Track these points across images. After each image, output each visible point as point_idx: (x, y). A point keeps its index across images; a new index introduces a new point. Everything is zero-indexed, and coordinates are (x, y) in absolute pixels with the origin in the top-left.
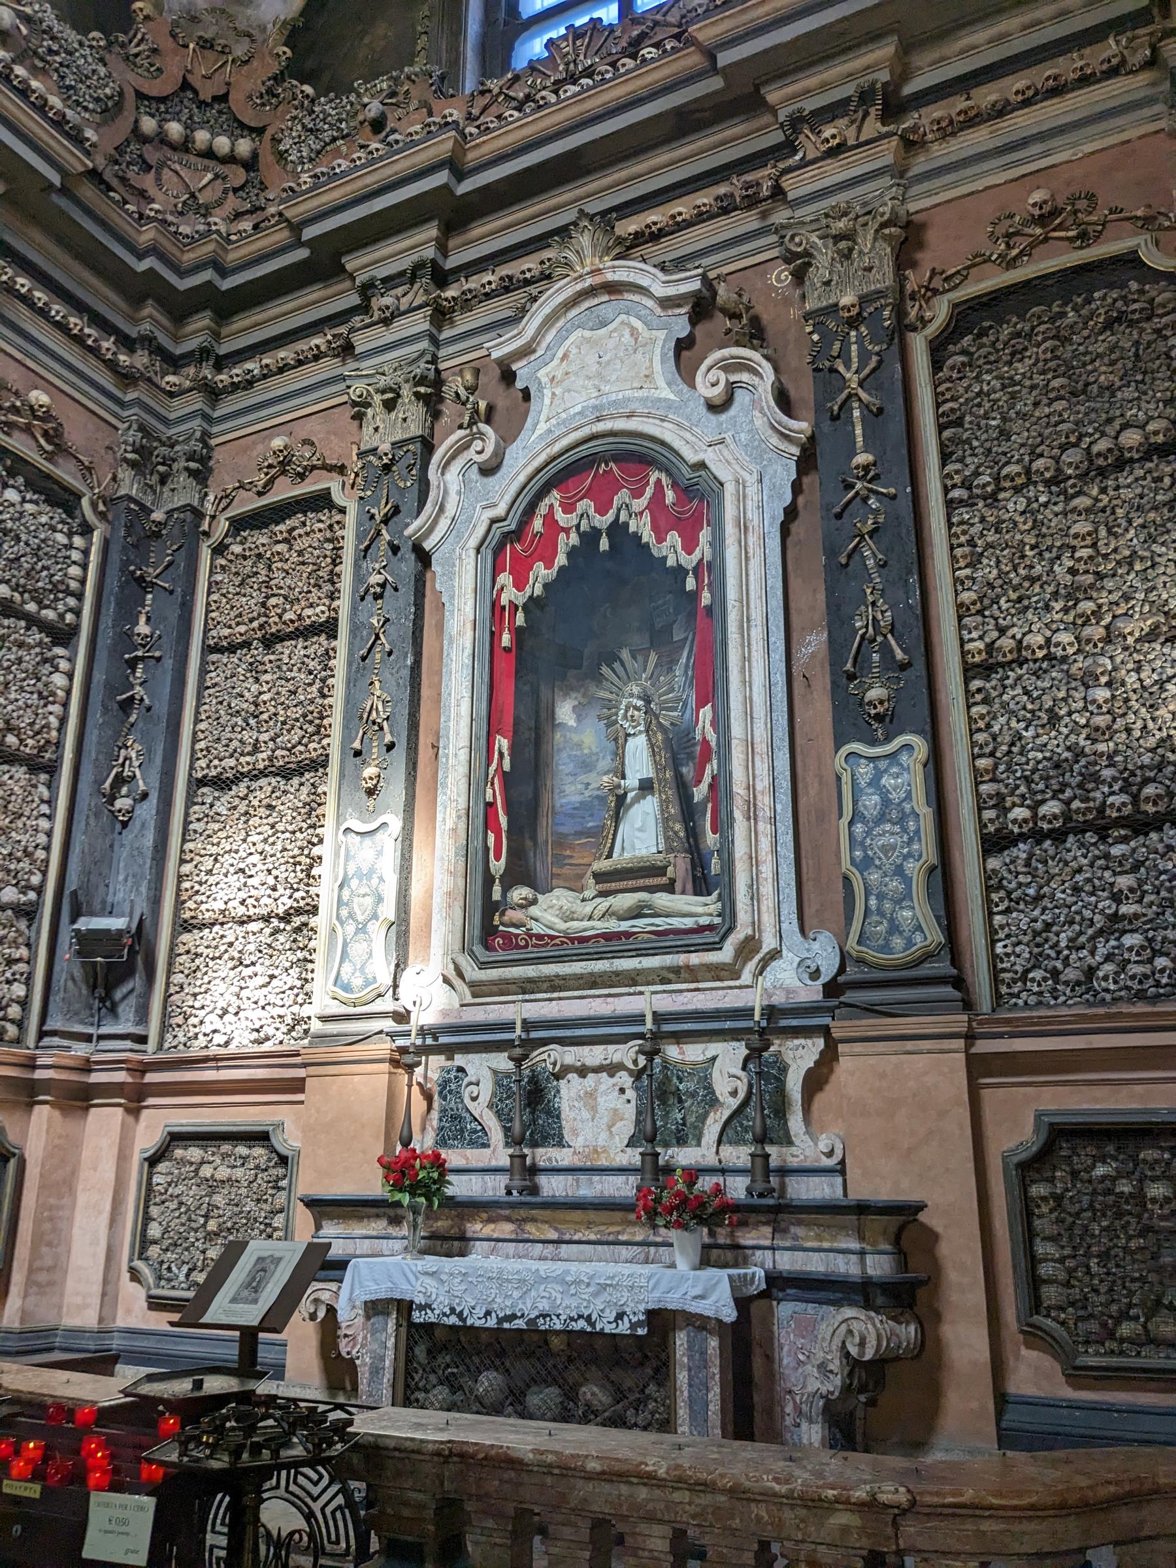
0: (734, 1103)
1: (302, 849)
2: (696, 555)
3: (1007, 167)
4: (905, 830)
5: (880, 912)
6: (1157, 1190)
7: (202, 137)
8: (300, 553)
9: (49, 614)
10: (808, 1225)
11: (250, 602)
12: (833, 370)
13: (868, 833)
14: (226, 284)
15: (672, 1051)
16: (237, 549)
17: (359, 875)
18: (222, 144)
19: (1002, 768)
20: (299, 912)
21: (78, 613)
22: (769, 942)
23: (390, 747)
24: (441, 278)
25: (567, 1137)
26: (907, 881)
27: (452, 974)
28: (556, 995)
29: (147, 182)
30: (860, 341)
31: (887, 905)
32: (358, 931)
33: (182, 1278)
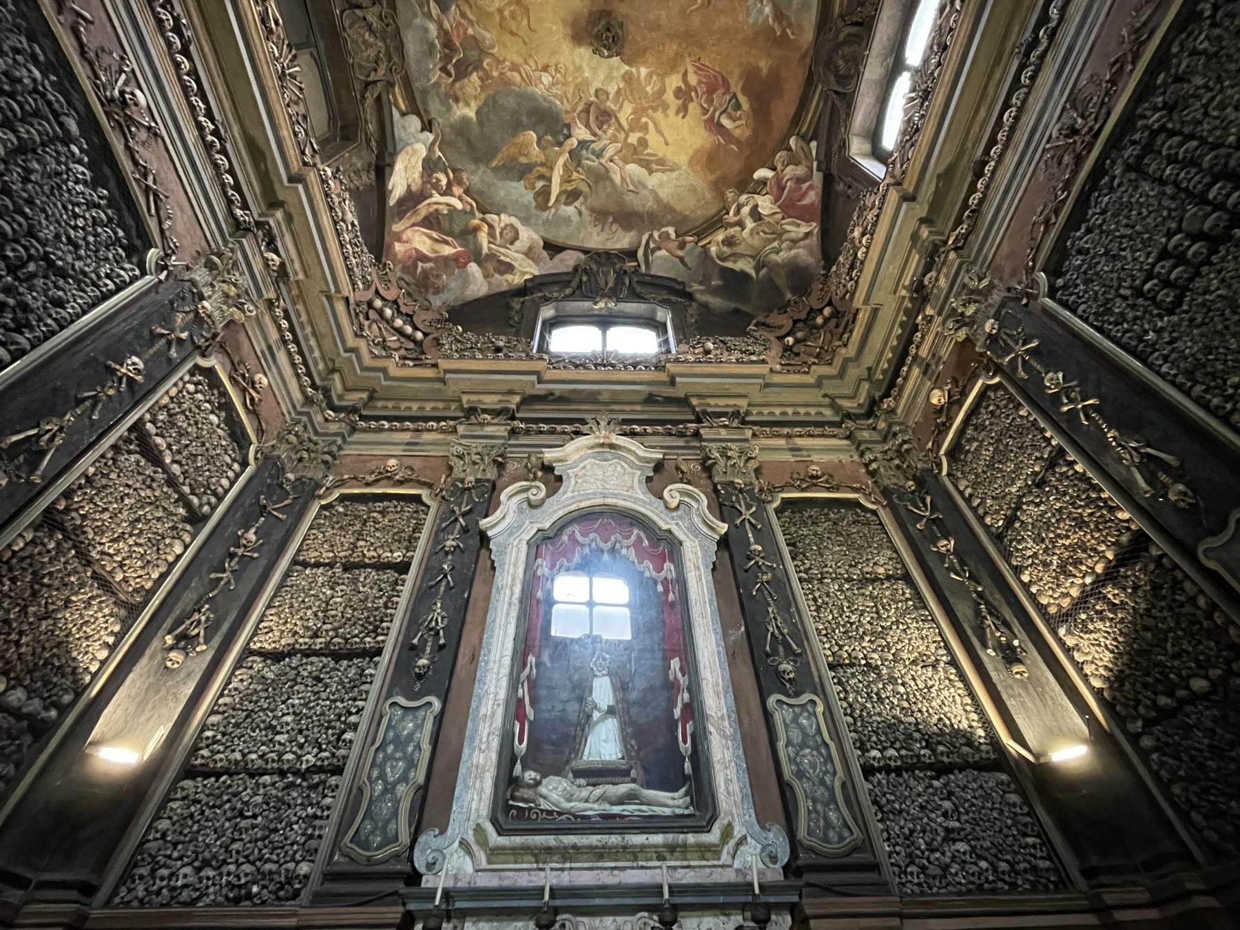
1: (340, 716)
2: (663, 574)
4: (821, 754)
5: (817, 812)
7: (399, 322)
9: (195, 500)
13: (797, 754)
16: (341, 509)
18: (409, 329)
19: (859, 724)
20: (320, 770)
21: (213, 508)
22: (738, 831)
23: (442, 647)
24: (513, 418)
26: (831, 790)
28: (568, 865)
30: (744, 498)
32: (385, 791)
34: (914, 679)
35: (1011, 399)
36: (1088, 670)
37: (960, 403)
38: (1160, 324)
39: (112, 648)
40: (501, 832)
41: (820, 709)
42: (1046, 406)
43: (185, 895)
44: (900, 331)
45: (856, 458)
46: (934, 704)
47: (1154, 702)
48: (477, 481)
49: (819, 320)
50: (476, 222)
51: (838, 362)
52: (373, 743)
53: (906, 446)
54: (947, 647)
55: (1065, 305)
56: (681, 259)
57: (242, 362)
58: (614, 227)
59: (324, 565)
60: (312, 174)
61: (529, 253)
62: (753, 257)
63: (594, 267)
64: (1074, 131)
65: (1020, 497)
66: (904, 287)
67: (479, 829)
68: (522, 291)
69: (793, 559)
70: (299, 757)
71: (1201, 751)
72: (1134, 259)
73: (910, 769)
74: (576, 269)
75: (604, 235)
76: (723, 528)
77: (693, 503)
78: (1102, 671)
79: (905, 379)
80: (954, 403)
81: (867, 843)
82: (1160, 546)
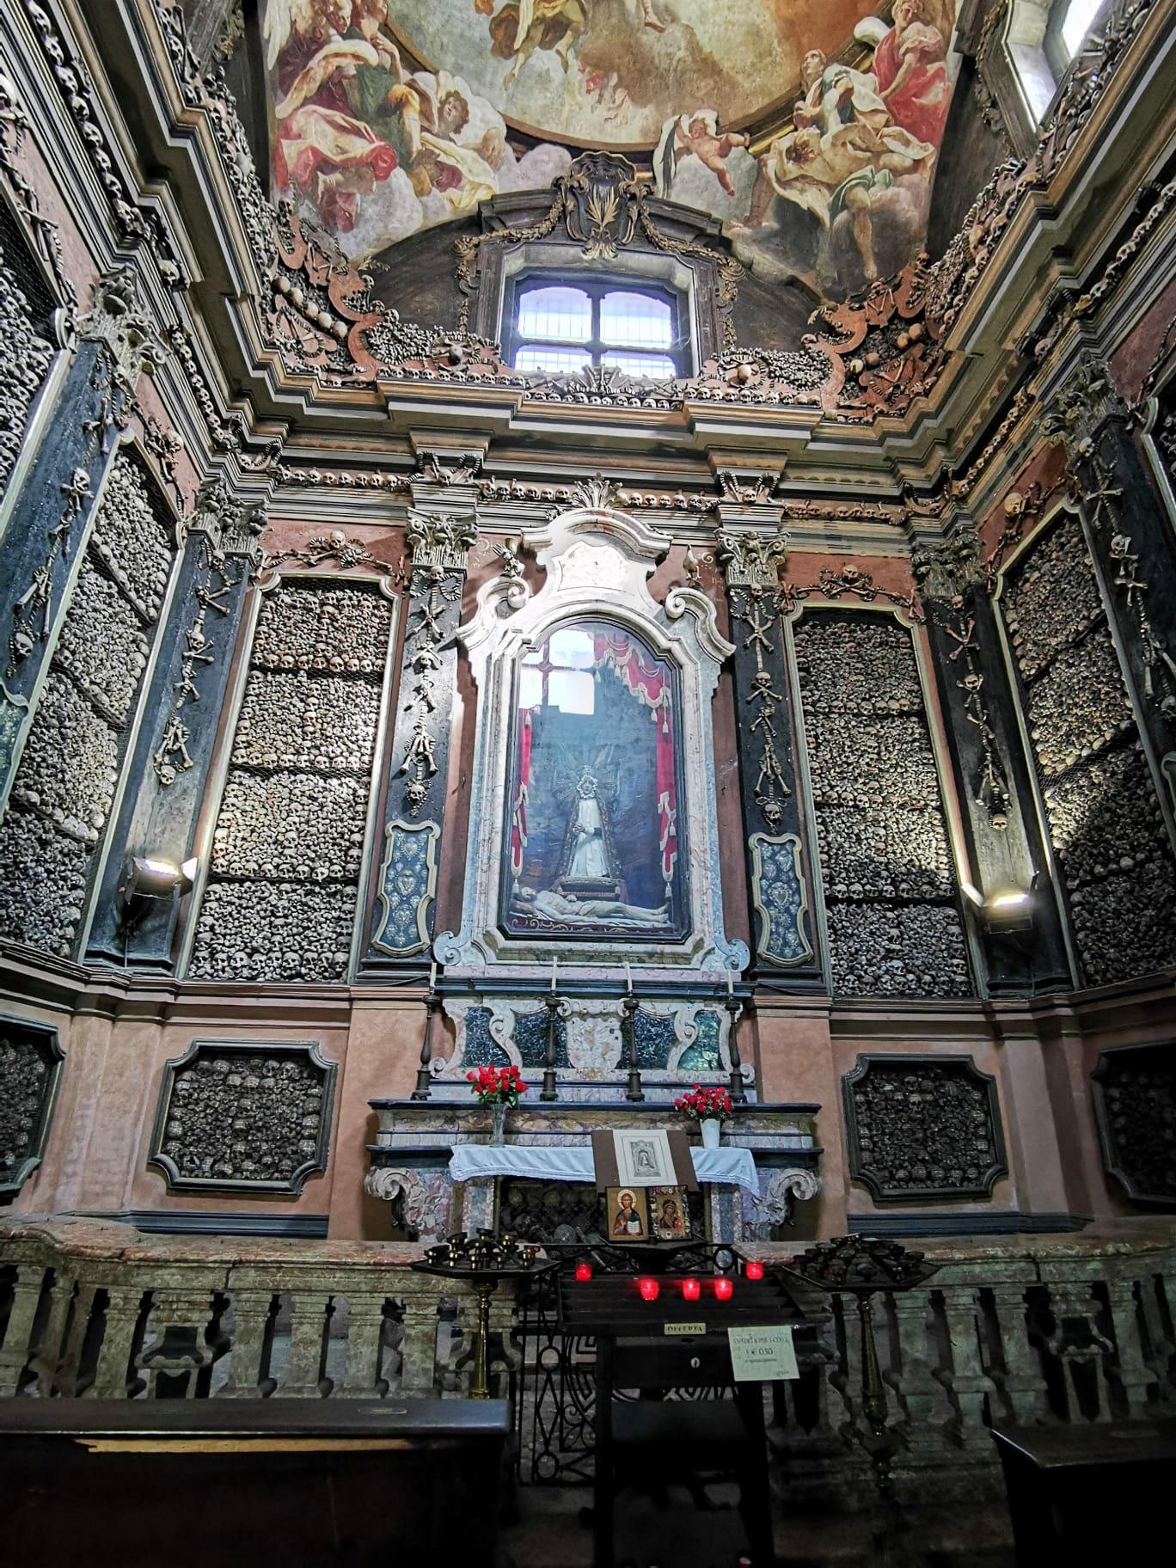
0: (689, 1042)
3: (830, 546)
6: (915, 1098)
8: (349, 619)
9: (142, 606)
10: (760, 1120)
11: (302, 641)
12: (745, 621)
14: (308, 411)
15: (646, 1006)
16: (288, 600)
17: (404, 859)
18: (327, 320)
20: (335, 881)
22: (707, 946)
25: (571, 1059)
26: (794, 917)
27: (482, 943)
29: (272, 318)
30: (760, 611)
31: (781, 930)
32: (401, 902)
33: (206, 1167)
34: (897, 822)
36: (1056, 832)
37: (1036, 519)
39: (118, 770)
40: (508, 937)
41: (797, 848)
43: (246, 972)
44: (996, 393)
45: (906, 554)
46: (910, 847)
47: (1092, 869)
48: (447, 570)
49: (902, 341)
50: (399, 89)
52: (382, 861)
53: (964, 552)
54: (939, 793)
56: (721, 175)
57: (152, 419)
58: (620, 94)
59: (288, 671)
60: (202, 122)
61: (483, 150)
62: (830, 187)
63: (585, 183)
65: (1058, 652)
66: (1014, 341)
67: (487, 935)
68: (475, 223)
69: (803, 687)
70: (312, 869)
73: (870, 901)
74: (557, 183)
75: (602, 111)
76: (731, 649)
77: (699, 612)
78: (1065, 836)
79: (988, 462)
81: (815, 959)
82: (1143, 744)
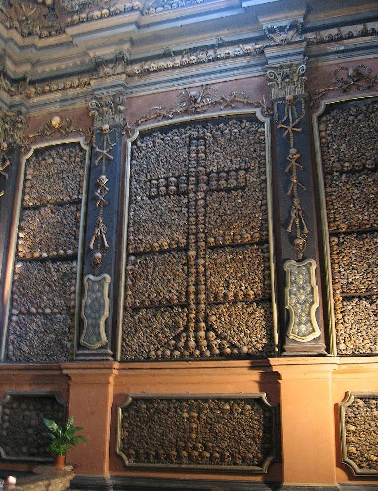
35: (83, 161)
37: (63, 136)
38: (144, 198)
42: (92, 185)
51: (28, 40)
53: (20, 126)
55: (132, 153)
64: (195, 101)
71: (30, 329)
72: (160, 169)
79: (50, 92)
80: (61, 132)
